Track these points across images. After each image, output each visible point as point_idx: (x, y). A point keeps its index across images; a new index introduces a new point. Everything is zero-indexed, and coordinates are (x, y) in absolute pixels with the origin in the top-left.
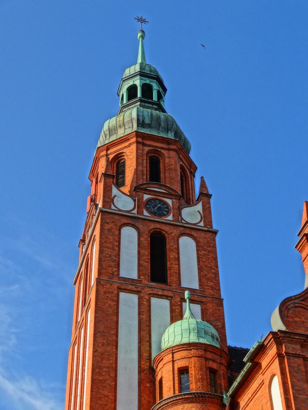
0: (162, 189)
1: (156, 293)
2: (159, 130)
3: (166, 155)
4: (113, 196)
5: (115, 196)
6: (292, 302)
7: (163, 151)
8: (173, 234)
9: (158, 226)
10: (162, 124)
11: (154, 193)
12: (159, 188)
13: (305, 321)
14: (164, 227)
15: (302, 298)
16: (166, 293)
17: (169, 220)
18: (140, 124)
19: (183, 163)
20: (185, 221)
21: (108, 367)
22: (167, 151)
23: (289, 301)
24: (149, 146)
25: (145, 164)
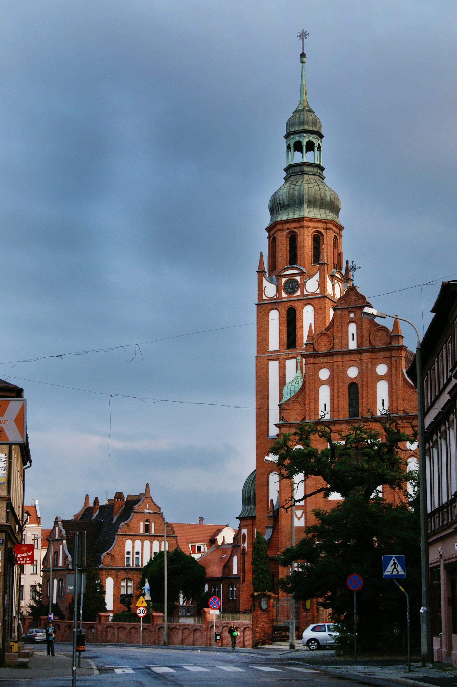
1: (288, 357)
2: (295, 206)
3: (298, 234)
5: (266, 287)
6: (291, 400)
7: (296, 230)
8: (299, 307)
9: (290, 304)
10: (297, 200)
14: (294, 304)
15: (297, 396)
16: (293, 355)
17: (298, 296)
18: (282, 207)
20: (308, 292)
24: (287, 229)
25: (285, 249)
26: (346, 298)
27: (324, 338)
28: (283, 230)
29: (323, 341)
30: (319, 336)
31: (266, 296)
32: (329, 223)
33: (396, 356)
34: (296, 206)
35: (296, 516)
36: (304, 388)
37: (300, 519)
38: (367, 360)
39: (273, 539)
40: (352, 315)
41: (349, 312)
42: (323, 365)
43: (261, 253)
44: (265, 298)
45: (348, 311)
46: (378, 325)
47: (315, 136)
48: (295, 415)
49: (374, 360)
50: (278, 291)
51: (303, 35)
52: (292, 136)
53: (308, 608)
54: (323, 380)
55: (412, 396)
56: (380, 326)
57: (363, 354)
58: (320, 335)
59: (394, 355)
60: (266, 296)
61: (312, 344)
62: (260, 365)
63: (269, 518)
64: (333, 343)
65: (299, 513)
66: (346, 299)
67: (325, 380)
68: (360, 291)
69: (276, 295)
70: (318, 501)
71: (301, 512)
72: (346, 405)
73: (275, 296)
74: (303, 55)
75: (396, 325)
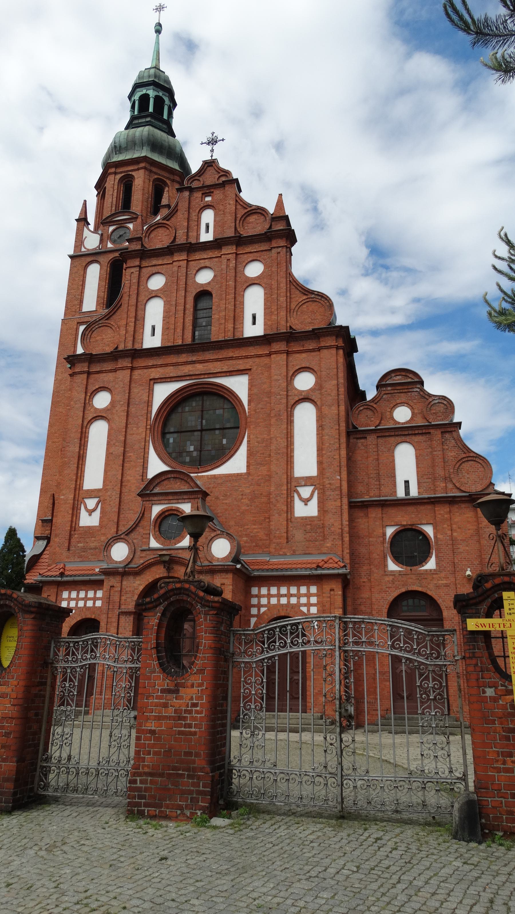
0: (126, 215)
3: (136, 177)
4: (84, 237)
5: (86, 237)
7: (133, 173)
10: (137, 142)
11: (117, 223)
12: (124, 215)
13: (105, 337)
19: (159, 175)
21: (64, 390)
22: (137, 172)
23: (94, 323)
24: (121, 173)
26: (199, 176)
27: (161, 231)
28: (115, 173)
29: (159, 236)
30: (153, 228)
31: (85, 248)
32: (176, 175)
33: (280, 247)
34: (136, 148)
35: (86, 507)
36: (121, 305)
37: (93, 514)
38: (230, 255)
39: (43, 556)
40: (208, 199)
41: (203, 194)
42: (154, 269)
43: (85, 201)
44: (83, 249)
45: (201, 193)
46: (250, 206)
47: (167, 94)
48: (101, 345)
49: (242, 256)
50: (101, 241)
51: (160, 8)
52: (138, 90)
53: (6, 664)
54: (153, 291)
55: (304, 306)
56: (253, 208)
57: (223, 247)
58: (155, 227)
59: (275, 246)
60: (85, 248)
61: (140, 239)
62: (67, 330)
63: (42, 522)
64: (174, 235)
65: (91, 503)
66: (201, 179)
67: (158, 290)
68: (223, 165)
69: (99, 246)
70: (129, 481)
71: (96, 500)
72: (188, 324)
73: (97, 247)
74: (159, 25)
75: (280, 204)
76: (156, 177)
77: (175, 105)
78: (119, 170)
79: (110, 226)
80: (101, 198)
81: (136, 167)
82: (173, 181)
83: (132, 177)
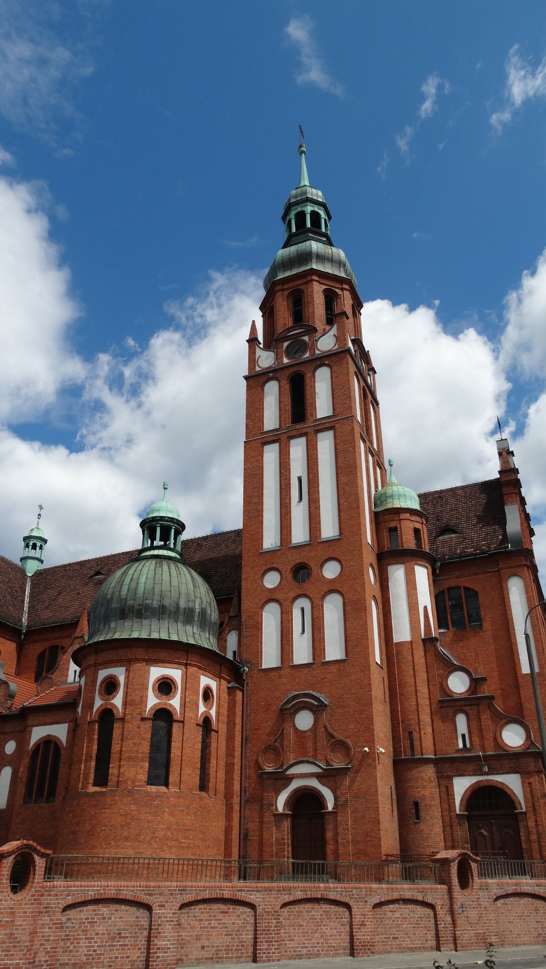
4: (257, 357)
5: (260, 356)
28: (283, 290)
31: (260, 367)
43: (254, 321)
44: (258, 369)
50: (278, 358)
60: (260, 367)
69: (274, 363)
76: (325, 287)
77: (330, 218)
78: (286, 287)
79: (284, 342)
80: (268, 317)
81: (304, 281)
82: (342, 289)
83: (302, 291)
